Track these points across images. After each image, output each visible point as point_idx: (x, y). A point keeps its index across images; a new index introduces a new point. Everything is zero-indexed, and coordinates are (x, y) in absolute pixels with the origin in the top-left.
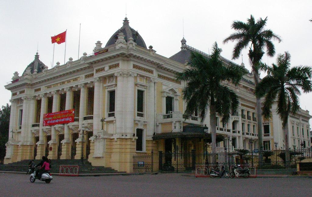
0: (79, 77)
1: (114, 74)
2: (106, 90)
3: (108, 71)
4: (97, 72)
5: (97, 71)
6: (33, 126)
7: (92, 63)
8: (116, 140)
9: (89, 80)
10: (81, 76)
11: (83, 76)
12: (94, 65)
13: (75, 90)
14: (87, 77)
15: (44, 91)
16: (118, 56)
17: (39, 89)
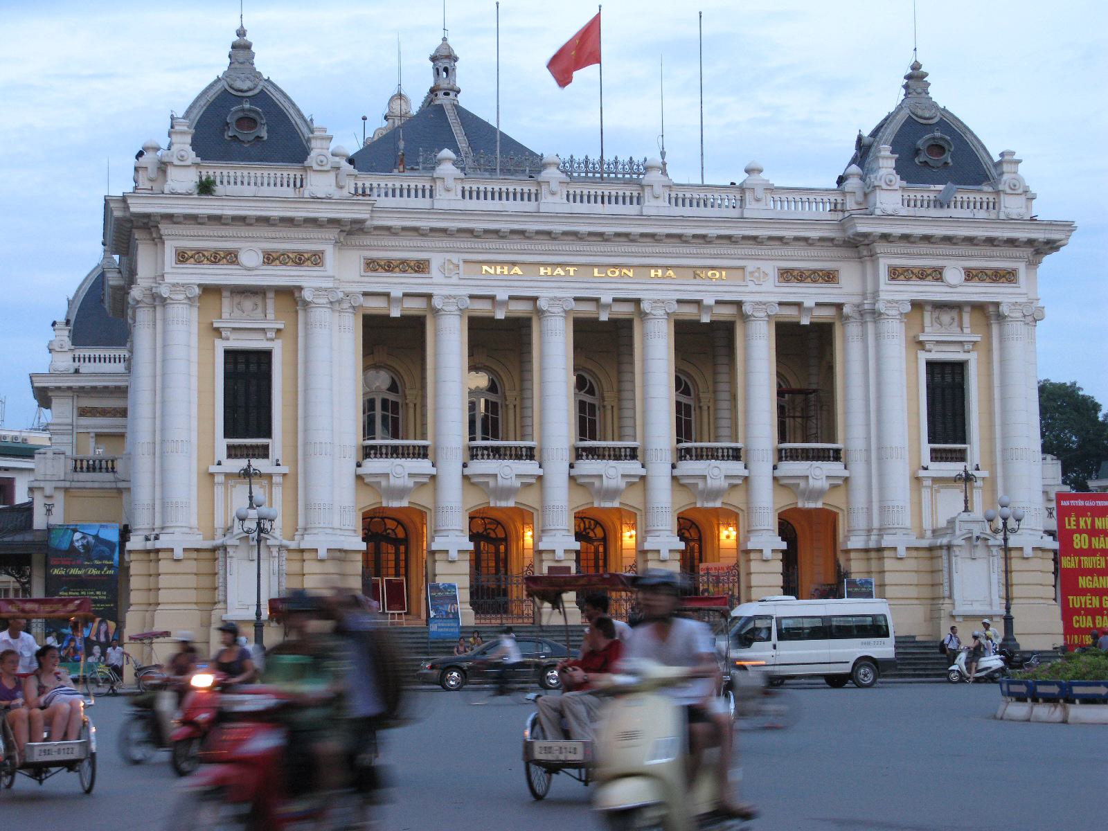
0: (743, 268)
1: (997, 304)
2: (923, 357)
3: (960, 289)
4: (893, 279)
5: (895, 274)
6: (368, 452)
7: (885, 237)
8: (1028, 552)
9: (810, 295)
10: (750, 265)
11: (770, 268)
12: (880, 248)
13: (697, 318)
14: (787, 275)
15: (455, 280)
16: (1030, 242)
17: (421, 267)
